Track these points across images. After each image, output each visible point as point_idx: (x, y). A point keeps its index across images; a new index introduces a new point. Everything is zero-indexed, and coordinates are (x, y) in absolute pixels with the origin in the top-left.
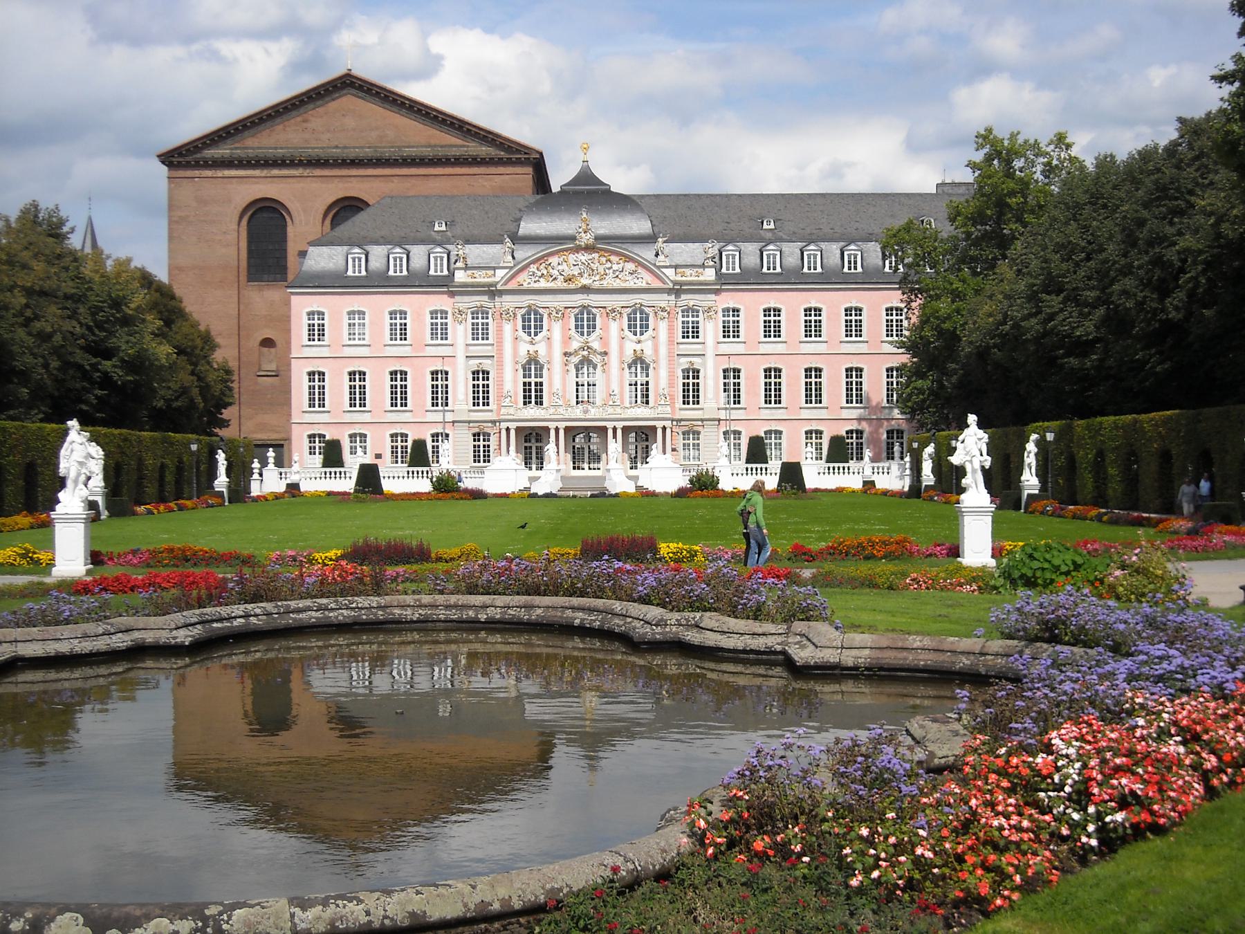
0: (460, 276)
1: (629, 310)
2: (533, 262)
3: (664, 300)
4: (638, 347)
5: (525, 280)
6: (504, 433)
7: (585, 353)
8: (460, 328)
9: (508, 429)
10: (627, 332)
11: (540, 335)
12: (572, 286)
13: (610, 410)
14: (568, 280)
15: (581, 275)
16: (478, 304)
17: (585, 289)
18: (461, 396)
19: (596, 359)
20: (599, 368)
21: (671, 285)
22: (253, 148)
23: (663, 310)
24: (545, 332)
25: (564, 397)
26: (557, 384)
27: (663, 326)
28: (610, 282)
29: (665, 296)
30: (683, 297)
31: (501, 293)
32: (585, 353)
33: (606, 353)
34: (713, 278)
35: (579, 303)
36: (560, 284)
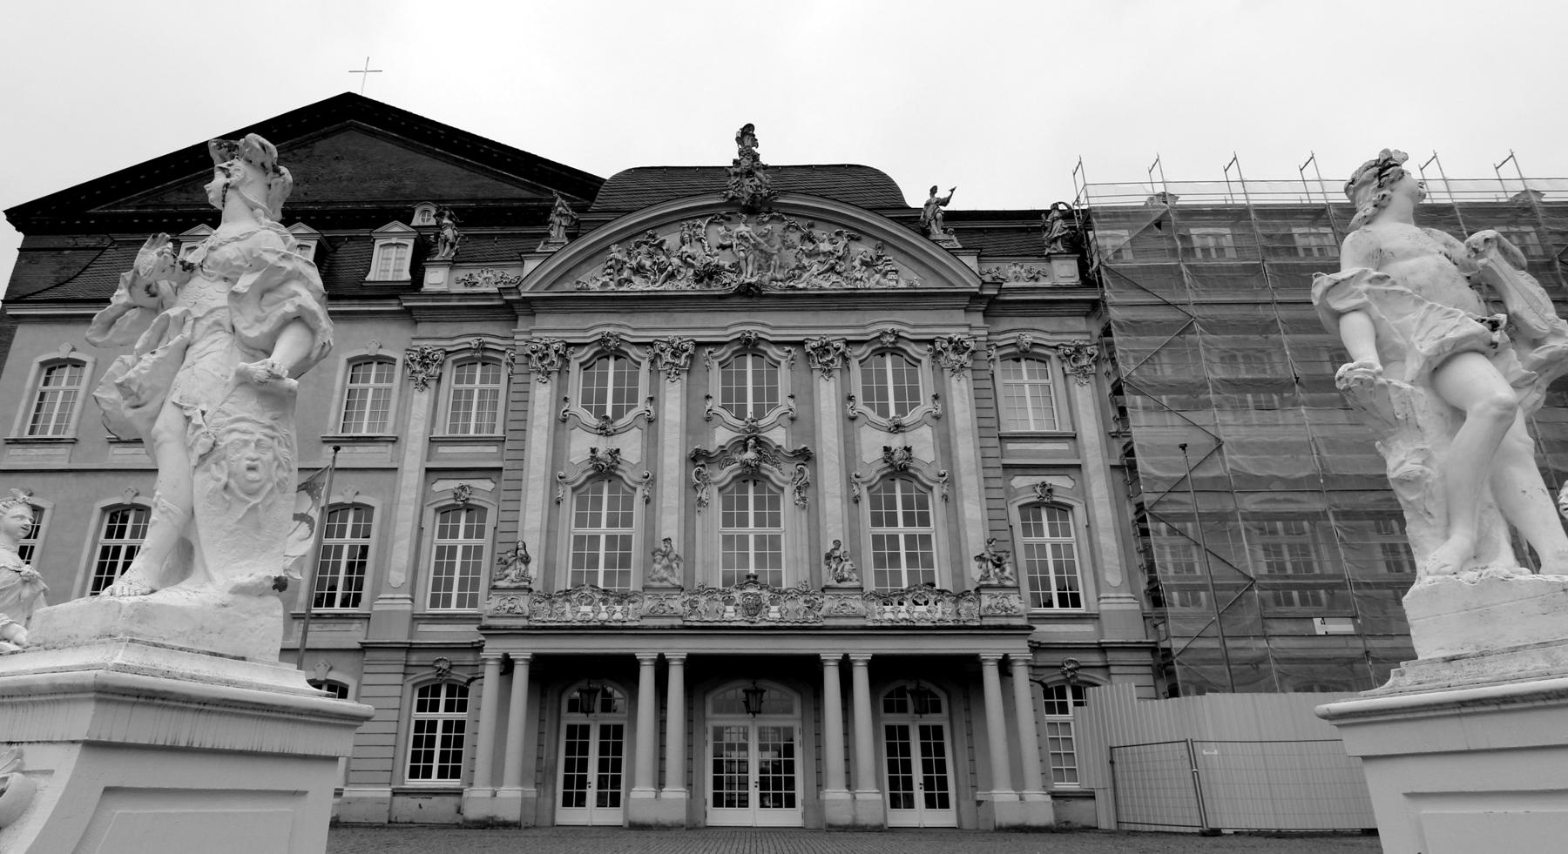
0: (436, 278)
1: (864, 351)
2: (624, 238)
3: (956, 325)
4: (896, 442)
5: (595, 280)
6: (491, 673)
7: (750, 455)
8: (421, 401)
9: (507, 665)
10: (860, 405)
11: (628, 418)
12: (716, 289)
13: (829, 603)
14: (708, 274)
15: (737, 268)
16: (474, 342)
17: (750, 295)
18: (398, 576)
19: (781, 474)
20: (787, 500)
21: (974, 286)
22: (175, 206)
23: (959, 347)
24: (641, 405)
25: (689, 575)
26: (670, 525)
27: (960, 391)
28: (814, 279)
29: (959, 316)
30: (1005, 324)
31: (531, 306)
32: (750, 455)
33: (805, 456)
34: (1075, 280)
35: (734, 332)
36: (684, 284)
